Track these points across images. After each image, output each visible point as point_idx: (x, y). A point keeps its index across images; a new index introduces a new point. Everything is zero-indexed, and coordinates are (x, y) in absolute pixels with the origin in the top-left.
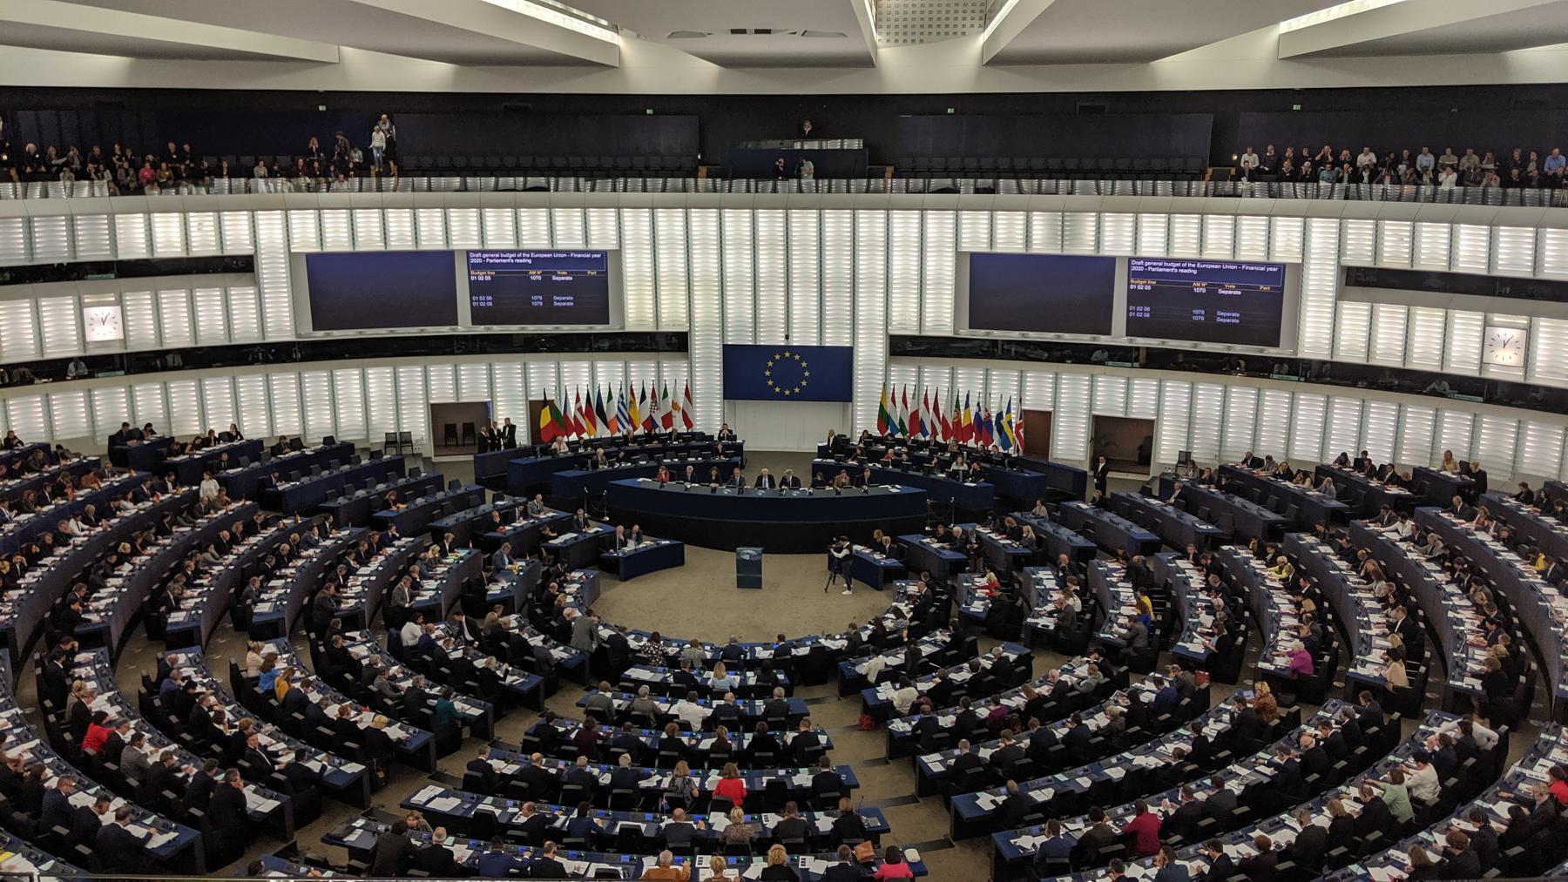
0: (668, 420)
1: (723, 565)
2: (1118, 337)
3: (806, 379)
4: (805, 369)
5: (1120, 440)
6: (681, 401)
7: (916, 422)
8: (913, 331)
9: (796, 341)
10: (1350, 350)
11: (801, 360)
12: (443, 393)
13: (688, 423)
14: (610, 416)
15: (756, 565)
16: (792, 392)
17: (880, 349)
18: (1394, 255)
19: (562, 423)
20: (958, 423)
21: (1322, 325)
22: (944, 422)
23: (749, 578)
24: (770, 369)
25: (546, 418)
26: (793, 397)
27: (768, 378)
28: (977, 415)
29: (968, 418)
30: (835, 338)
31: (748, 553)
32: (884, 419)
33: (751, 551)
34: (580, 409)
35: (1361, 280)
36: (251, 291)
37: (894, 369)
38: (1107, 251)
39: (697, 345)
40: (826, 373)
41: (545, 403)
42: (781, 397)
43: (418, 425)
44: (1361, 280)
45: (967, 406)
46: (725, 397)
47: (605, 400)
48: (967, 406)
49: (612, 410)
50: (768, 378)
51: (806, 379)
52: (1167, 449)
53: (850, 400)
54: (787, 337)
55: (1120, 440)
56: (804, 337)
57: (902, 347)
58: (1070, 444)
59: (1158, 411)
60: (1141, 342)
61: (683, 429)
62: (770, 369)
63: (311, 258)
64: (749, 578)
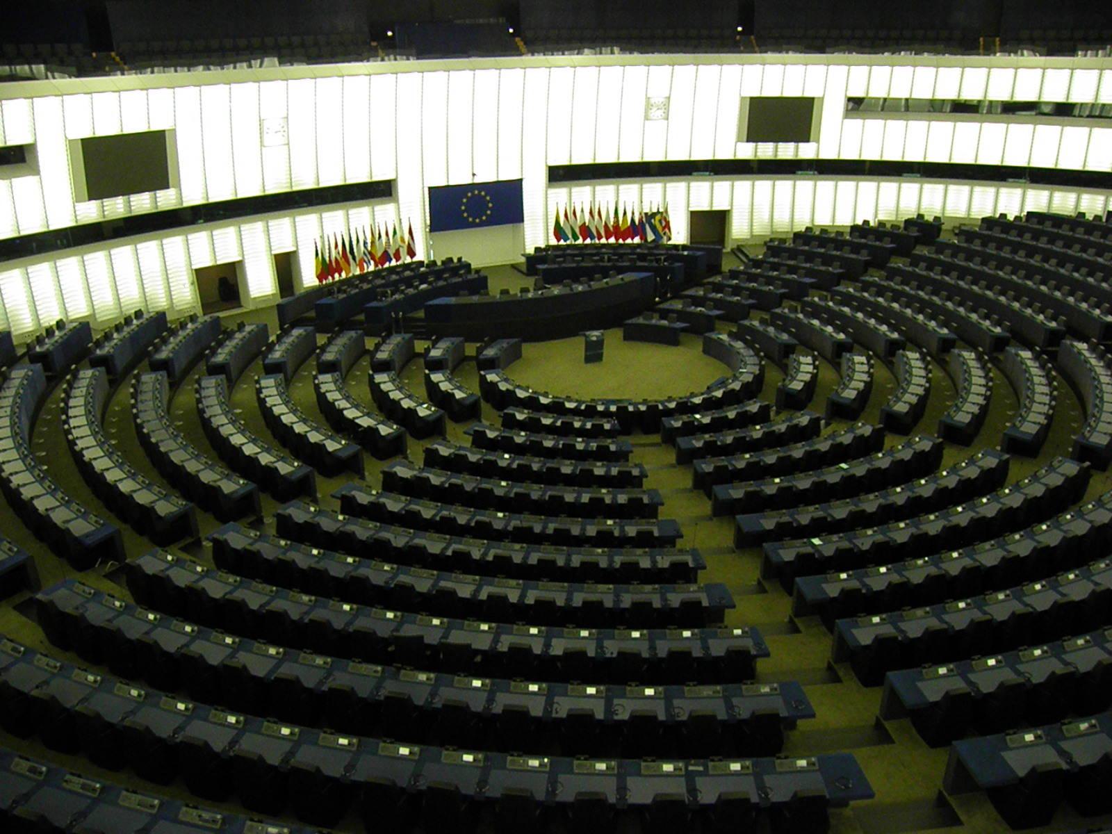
0: (398, 257)
1: (574, 347)
5: (711, 224)
6: (407, 237)
7: (586, 231)
8: (564, 161)
9: (478, 180)
10: (850, 154)
11: (486, 195)
12: (204, 261)
14: (357, 260)
15: (600, 344)
16: (481, 220)
17: (543, 176)
18: (878, 92)
20: (616, 226)
22: (606, 226)
23: (594, 354)
28: (633, 220)
29: (625, 224)
30: (507, 175)
31: (594, 335)
32: (559, 232)
33: (596, 333)
35: (857, 106)
37: (552, 191)
39: (402, 190)
40: (499, 203)
43: (185, 295)
44: (857, 106)
45: (625, 213)
47: (354, 243)
48: (625, 213)
49: (359, 251)
52: (739, 229)
54: (474, 175)
55: (711, 224)
56: (486, 175)
57: (560, 175)
58: (679, 234)
59: (732, 206)
61: (408, 260)
64: (594, 354)
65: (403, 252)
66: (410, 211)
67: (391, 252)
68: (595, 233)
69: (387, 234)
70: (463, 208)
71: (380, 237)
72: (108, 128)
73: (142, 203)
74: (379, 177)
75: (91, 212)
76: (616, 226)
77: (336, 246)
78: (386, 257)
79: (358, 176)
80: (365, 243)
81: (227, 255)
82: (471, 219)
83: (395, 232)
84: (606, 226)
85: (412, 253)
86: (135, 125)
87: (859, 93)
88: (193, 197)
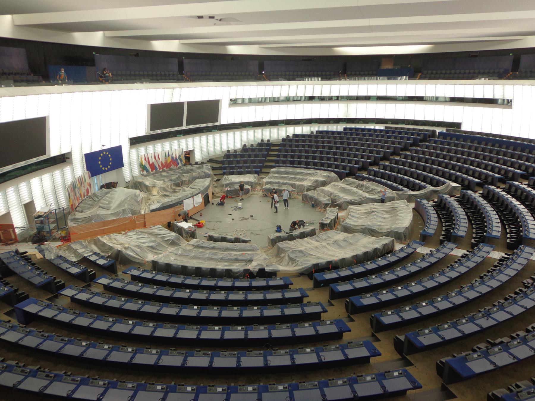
2: (184, 128)
3: (111, 161)
21: (227, 115)
24: (100, 160)
26: (109, 170)
27: (100, 165)
29: (169, 160)
35: (234, 102)
38: (181, 101)
42: (105, 171)
44: (234, 102)
50: (100, 165)
51: (111, 161)
52: (198, 157)
53: (123, 166)
57: (135, 142)
60: (190, 127)
62: (100, 160)
66: (78, 168)
68: (158, 167)
70: (100, 162)
76: (166, 163)
82: (103, 169)
84: (162, 163)
87: (233, 97)
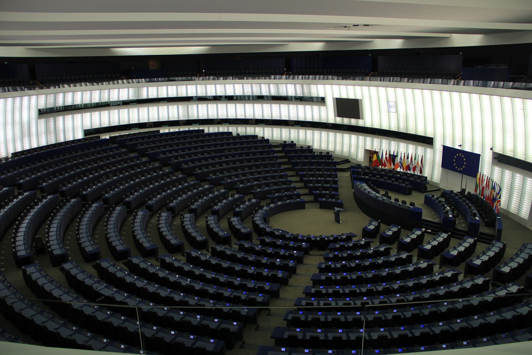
0: (414, 170)
3: (465, 165)
4: (465, 161)
6: (420, 163)
12: (369, 148)
13: (421, 172)
14: (396, 163)
19: (380, 161)
25: (375, 158)
26: (460, 172)
34: (386, 158)
36: (325, 107)
41: (376, 153)
42: (456, 171)
43: (360, 157)
46: (442, 166)
56: (467, 148)
63: (337, 98)
65: (418, 169)
67: (411, 167)
69: (412, 158)
71: (408, 158)
72: (344, 96)
73: (353, 122)
74: (429, 135)
75: (339, 120)
77: (386, 154)
78: (408, 168)
79: (420, 132)
80: (401, 159)
81: (376, 148)
83: (415, 159)
85: (421, 172)
86: (352, 97)
88: (368, 125)
